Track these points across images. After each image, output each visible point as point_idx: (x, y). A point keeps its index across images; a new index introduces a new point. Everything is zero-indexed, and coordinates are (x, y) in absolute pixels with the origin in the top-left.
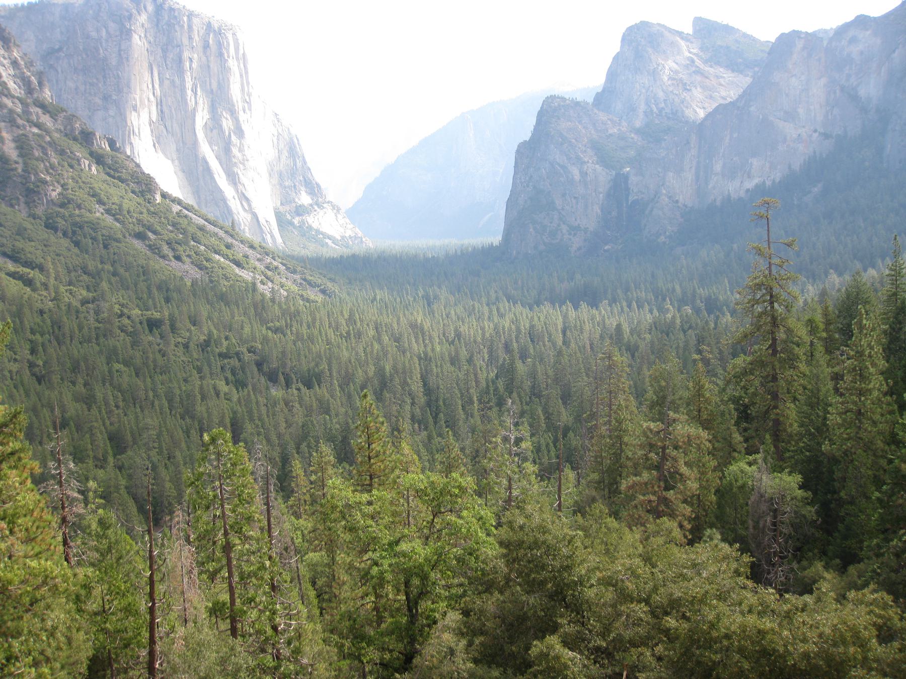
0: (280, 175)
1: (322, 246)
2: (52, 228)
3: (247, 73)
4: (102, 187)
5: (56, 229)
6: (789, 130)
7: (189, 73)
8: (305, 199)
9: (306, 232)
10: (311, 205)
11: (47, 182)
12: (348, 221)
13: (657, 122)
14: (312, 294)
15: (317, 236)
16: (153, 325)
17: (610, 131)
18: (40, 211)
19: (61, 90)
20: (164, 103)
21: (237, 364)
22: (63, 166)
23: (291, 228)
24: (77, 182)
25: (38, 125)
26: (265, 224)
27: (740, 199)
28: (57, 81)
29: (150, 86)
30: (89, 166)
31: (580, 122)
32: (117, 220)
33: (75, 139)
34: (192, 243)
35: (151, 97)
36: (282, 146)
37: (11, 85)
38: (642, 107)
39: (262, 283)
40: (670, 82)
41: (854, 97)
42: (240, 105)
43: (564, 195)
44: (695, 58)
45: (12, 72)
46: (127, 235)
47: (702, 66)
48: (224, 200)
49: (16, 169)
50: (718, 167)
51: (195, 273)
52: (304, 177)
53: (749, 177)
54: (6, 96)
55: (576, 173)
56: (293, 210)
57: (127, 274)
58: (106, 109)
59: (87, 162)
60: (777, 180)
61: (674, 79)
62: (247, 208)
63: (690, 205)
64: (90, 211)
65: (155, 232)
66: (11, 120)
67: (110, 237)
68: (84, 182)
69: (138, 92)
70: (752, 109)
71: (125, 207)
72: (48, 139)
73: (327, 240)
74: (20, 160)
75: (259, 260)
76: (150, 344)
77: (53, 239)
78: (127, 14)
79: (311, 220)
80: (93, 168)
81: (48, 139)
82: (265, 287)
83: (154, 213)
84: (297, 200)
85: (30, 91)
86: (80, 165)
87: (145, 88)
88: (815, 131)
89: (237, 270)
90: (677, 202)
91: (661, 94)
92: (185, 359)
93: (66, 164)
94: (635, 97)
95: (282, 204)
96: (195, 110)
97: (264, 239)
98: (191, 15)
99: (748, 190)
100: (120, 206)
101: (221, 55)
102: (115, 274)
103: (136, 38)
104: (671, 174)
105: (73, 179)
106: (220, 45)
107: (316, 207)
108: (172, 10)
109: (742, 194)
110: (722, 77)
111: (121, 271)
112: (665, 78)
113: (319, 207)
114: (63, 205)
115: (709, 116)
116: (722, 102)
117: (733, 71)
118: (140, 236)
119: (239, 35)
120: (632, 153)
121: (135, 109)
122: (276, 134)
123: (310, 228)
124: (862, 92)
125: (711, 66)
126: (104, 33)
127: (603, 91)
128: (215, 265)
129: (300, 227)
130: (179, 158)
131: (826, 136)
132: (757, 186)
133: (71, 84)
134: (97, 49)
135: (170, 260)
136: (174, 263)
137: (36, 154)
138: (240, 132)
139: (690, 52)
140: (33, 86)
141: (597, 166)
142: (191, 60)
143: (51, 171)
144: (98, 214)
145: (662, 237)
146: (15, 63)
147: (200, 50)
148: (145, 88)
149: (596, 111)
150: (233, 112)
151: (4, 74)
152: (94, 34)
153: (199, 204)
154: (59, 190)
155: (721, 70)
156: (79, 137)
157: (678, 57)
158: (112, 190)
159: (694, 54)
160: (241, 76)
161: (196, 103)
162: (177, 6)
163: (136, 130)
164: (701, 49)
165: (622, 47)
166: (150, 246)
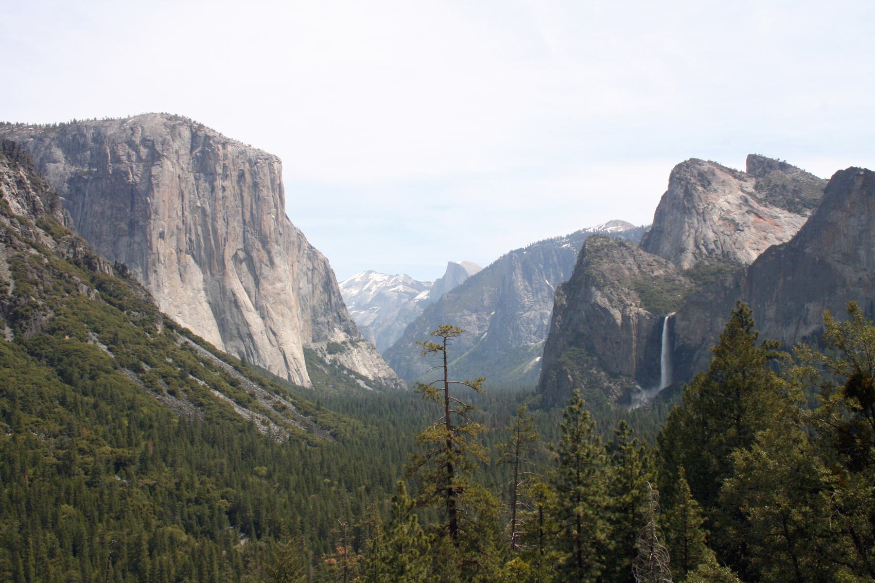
0: (314, 309)
1: (353, 386)
2: (36, 355)
3: (282, 203)
4: (99, 315)
5: (39, 356)
7: (221, 202)
8: (340, 336)
9: (337, 370)
10: (344, 343)
11: (37, 306)
12: (382, 361)
13: (707, 263)
14: (317, 438)
15: (349, 376)
16: (119, 465)
17: (656, 273)
18: (27, 336)
19: (86, 213)
20: (193, 231)
21: (207, 512)
22: (58, 290)
23: (320, 367)
24: (72, 308)
25: (34, 247)
26: (292, 361)
28: (83, 206)
29: (180, 214)
30: (89, 291)
31: (624, 263)
32: (110, 349)
33: (77, 264)
34: (191, 377)
35: (181, 225)
36: (316, 280)
37: (14, 205)
39: (264, 423)
40: (721, 222)
42: (273, 236)
43: (605, 339)
44: (749, 198)
45: (16, 190)
46: (118, 366)
47: (755, 205)
48: (250, 336)
49: (6, 292)
51: (189, 409)
52: (338, 313)
53: (805, 323)
54: (5, 215)
55: (617, 315)
56: (325, 347)
57: (109, 407)
58: (131, 235)
59: (85, 287)
61: (726, 219)
62: (275, 343)
64: (81, 339)
65: (152, 366)
66: (8, 240)
67: (99, 368)
68: (78, 309)
69: (166, 218)
70: (807, 250)
71: (121, 335)
72: (46, 261)
73: (359, 381)
74: (12, 282)
75: (265, 398)
76: (111, 485)
77: (33, 367)
78: (161, 139)
79: (342, 358)
80: (93, 296)
81: (46, 261)
82: (266, 428)
83: (153, 344)
84: (329, 337)
85: (34, 210)
86: (78, 290)
87: (174, 216)
89: (238, 410)
91: (711, 235)
92: (146, 502)
93: (61, 288)
94: (684, 238)
95: (314, 341)
96: (225, 240)
97: (289, 376)
98: (225, 143)
100: (116, 334)
101: (255, 185)
102: (95, 406)
103: (167, 164)
105: (67, 304)
106: (254, 174)
107: (350, 346)
108: (207, 137)
110: (779, 217)
111: (103, 405)
112: (716, 218)
113: (353, 346)
114: (52, 331)
115: (760, 257)
118: (137, 369)
119: (276, 165)
121: (162, 236)
122: (311, 268)
123: (342, 367)
125: (766, 206)
126: (134, 158)
127: (652, 231)
128: (212, 402)
129: (331, 365)
130: (205, 290)
133: (97, 208)
134: (127, 174)
135: (164, 395)
136: (169, 399)
137: (30, 276)
138: (272, 263)
139: (743, 191)
140: (37, 207)
141: (640, 309)
142: (224, 189)
143: (44, 295)
144: (91, 343)
146: (20, 183)
147: (235, 178)
148: (174, 216)
149: (641, 252)
150: (265, 242)
151: (6, 193)
152: (124, 158)
154: (51, 314)
156: (82, 261)
157: (730, 196)
158: (112, 318)
159: (750, 194)
160: (276, 206)
161: (227, 233)
162: (211, 134)
163: (162, 258)
164: (756, 187)
165: (670, 186)
166: (142, 379)
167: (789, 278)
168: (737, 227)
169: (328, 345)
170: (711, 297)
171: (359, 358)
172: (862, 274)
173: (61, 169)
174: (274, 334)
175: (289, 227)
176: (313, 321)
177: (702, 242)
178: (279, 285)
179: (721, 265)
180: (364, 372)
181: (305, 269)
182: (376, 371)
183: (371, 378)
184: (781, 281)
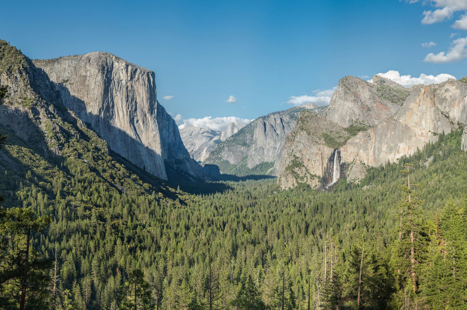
6: (418, 131)
8: (181, 156)
13: (355, 125)
17: (332, 130)
27: (394, 163)
38: (348, 118)
41: (448, 117)
43: (309, 160)
50: (384, 148)
53: (398, 153)
56: (174, 161)
60: (412, 155)
63: (371, 165)
70: (401, 121)
88: (430, 131)
90: (365, 164)
99: (398, 159)
104: (361, 151)
107: (185, 160)
109: (395, 161)
112: (360, 104)
116: (386, 116)
117: (393, 102)
120: (342, 140)
124: (451, 115)
131: (435, 134)
132: (402, 157)
141: (325, 146)
145: (357, 181)
152: (84, 74)
153: (128, 157)
155: (386, 101)
167: (393, 133)
168: (369, 110)
169: (175, 160)
170: (357, 141)
171: (190, 167)
172: (423, 131)
173: (55, 79)
174: (152, 156)
175: (158, 104)
176: (169, 150)
177: (353, 115)
178: (154, 133)
179: (362, 126)
180: (192, 173)
181: (165, 125)
182: (198, 173)
183: (195, 176)
184: (389, 134)
